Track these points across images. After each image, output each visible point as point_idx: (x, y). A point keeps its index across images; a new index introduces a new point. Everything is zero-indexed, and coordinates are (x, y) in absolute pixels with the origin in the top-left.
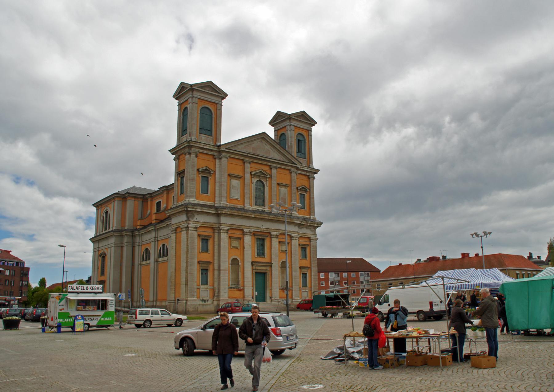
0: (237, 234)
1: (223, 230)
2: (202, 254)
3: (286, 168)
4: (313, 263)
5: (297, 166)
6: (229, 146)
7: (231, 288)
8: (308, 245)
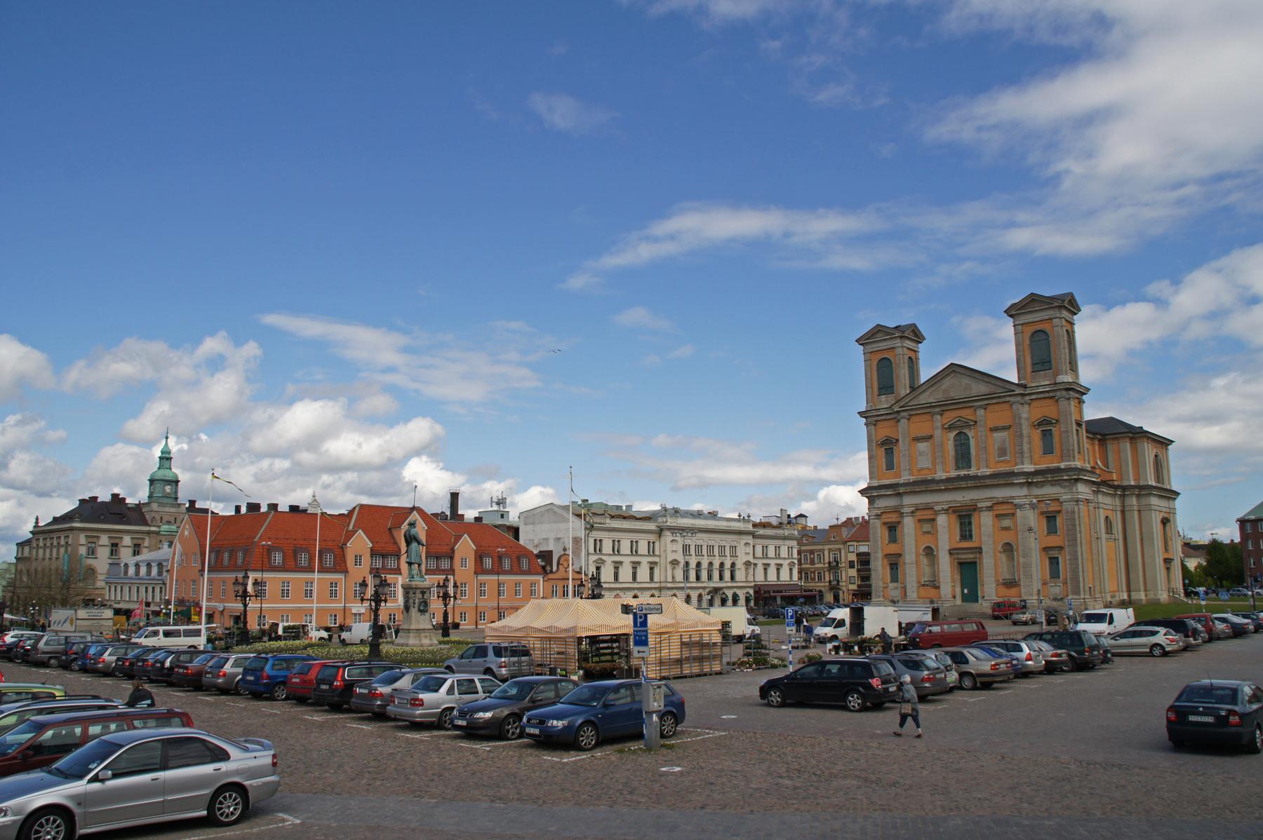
0: (927, 515)
1: (906, 513)
2: (890, 545)
3: (1001, 400)
4: (1069, 541)
5: (1016, 393)
6: (904, 403)
7: (923, 585)
8: (1059, 512)
